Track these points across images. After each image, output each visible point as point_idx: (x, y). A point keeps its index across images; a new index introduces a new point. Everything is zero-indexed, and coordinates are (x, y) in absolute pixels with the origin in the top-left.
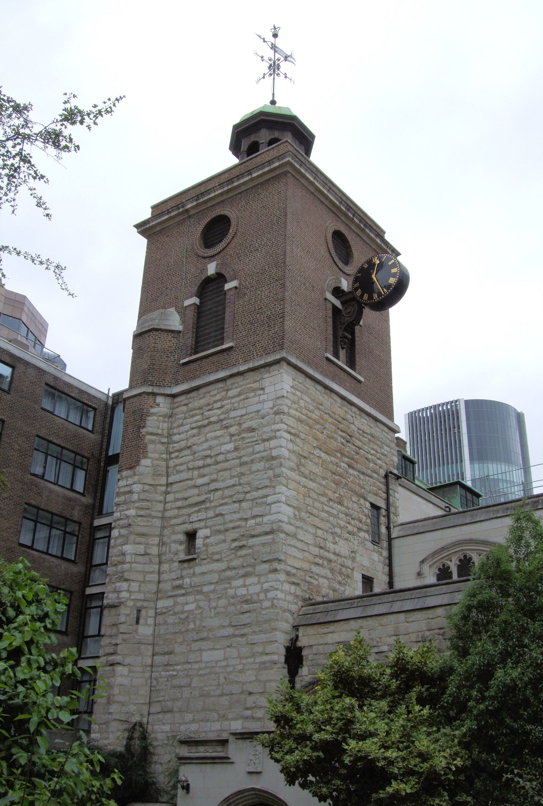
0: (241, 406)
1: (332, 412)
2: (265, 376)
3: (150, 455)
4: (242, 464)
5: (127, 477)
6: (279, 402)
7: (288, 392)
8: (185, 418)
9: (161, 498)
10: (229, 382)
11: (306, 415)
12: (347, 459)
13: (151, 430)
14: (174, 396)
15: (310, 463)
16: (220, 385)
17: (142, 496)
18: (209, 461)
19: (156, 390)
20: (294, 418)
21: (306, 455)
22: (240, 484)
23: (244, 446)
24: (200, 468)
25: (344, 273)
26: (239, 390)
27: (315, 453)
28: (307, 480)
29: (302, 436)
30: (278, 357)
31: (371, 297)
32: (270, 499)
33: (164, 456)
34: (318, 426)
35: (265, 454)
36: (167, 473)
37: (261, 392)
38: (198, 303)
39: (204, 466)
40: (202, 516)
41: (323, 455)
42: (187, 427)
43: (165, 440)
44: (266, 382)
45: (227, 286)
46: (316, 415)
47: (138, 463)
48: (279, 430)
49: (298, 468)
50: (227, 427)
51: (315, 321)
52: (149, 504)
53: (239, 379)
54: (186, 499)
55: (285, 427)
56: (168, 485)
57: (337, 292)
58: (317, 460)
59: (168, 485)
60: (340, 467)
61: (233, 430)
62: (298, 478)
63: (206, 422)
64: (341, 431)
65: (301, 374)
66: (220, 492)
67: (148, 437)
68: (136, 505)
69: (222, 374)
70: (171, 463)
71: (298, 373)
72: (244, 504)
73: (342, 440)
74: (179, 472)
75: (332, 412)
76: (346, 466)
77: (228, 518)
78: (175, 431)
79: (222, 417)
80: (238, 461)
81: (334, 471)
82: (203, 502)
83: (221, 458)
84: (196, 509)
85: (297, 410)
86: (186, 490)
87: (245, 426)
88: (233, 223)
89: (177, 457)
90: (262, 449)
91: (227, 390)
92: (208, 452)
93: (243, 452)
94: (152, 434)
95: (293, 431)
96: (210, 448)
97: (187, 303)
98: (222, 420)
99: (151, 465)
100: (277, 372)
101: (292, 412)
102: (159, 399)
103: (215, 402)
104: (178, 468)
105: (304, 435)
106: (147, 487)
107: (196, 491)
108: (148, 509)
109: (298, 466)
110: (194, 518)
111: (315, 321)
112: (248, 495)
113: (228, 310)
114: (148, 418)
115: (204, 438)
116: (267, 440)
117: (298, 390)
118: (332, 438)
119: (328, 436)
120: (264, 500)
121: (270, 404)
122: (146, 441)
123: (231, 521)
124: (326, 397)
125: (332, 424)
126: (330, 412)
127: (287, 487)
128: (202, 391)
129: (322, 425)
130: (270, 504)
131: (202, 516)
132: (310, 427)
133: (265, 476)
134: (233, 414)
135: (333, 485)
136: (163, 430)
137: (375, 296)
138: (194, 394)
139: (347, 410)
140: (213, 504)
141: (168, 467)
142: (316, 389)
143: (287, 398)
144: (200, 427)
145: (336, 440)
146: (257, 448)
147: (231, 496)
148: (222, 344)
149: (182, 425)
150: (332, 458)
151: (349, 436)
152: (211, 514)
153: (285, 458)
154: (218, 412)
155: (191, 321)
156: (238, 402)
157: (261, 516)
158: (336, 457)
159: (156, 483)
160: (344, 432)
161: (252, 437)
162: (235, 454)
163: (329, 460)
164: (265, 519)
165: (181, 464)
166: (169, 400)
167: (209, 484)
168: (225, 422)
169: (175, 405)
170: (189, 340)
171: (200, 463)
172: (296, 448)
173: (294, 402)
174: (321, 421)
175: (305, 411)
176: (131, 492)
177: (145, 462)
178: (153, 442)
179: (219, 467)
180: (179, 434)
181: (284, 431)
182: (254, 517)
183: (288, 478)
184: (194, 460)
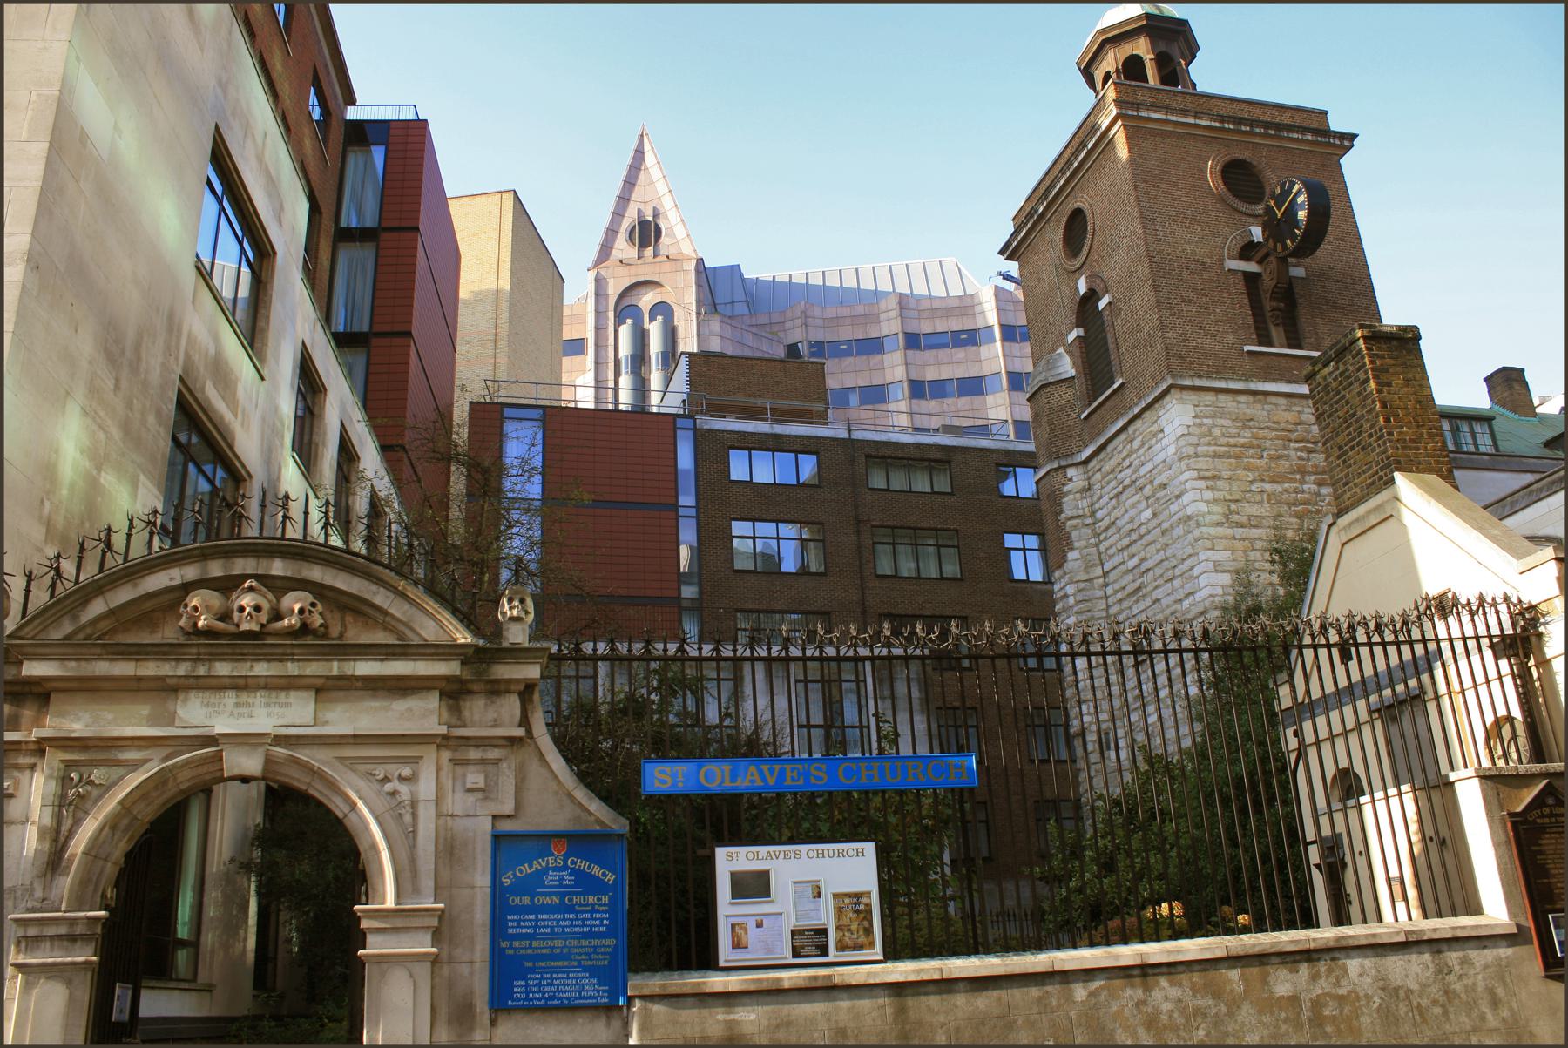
0: (1148, 458)
1: (1274, 422)
2: (1161, 414)
3: (1076, 545)
4: (1164, 533)
5: (1060, 579)
6: (1182, 442)
7: (1189, 426)
8: (1102, 488)
9: (1101, 593)
10: (1131, 429)
11: (1228, 445)
12: (1313, 478)
13: (1069, 514)
14: (1086, 462)
15: (1247, 505)
16: (1123, 436)
17: (1079, 597)
18: (1134, 536)
19: (1063, 463)
20: (1207, 456)
21: (1238, 497)
22: (1167, 559)
23: (1161, 508)
24: (1128, 546)
25: (1256, 216)
26: (1141, 438)
27: (1253, 489)
28: (1247, 529)
29: (1226, 474)
30: (1164, 386)
31: (1285, 247)
32: (1196, 572)
33: (1093, 541)
34: (1252, 451)
35: (1181, 514)
36: (1101, 560)
37: (1161, 435)
38: (1082, 334)
39: (1131, 544)
40: (1141, 606)
41: (1268, 487)
42: (1106, 499)
43: (1088, 521)
44: (1163, 422)
45: (1102, 304)
46: (1244, 437)
47: (1064, 559)
48: (1187, 481)
49: (1228, 519)
50: (1141, 489)
51: (1218, 310)
52: (1089, 604)
53: (1138, 423)
54: (1124, 588)
55: (1195, 474)
56: (1105, 575)
57: (1247, 250)
58: (1259, 498)
59: (1105, 575)
60: (1303, 492)
61: (1147, 491)
62: (1229, 532)
63: (1121, 487)
64: (1297, 441)
65: (1206, 393)
66: (1151, 572)
67: (1069, 523)
68: (1076, 609)
69: (1120, 424)
70: (1102, 548)
71: (1202, 394)
72: (1177, 583)
73: (1299, 453)
74: (1111, 557)
75: (1274, 422)
76: (1315, 487)
77: (1164, 602)
78: (1097, 506)
79: (1133, 478)
80: (1158, 530)
81: (1292, 501)
82: (1139, 588)
83: (1143, 530)
84: (1135, 598)
85: (1209, 444)
86: (1121, 577)
87: (1156, 483)
88: (1089, 217)
89: (1106, 539)
90: (1177, 509)
91: (1131, 441)
92: (1130, 526)
93: (1161, 518)
94: (1072, 518)
95: (1208, 474)
96: (1132, 520)
97: (1071, 337)
98: (1134, 482)
99: (1079, 557)
100: (1170, 405)
101: (1201, 449)
102: (1071, 472)
103: (1124, 459)
104: (1111, 552)
105: (1229, 473)
106: (1082, 585)
107: (1130, 577)
108: (1089, 611)
109: (1226, 516)
110: (1135, 611)
111: (1218, 310)
112: (1176, 570)
113: (1109, 336)
114: (1064, 500)
115: (1123, 510)
116: (1178, 497)
117: (1207, 417)
118: (1280, 457)
119: (1271, 458)
120: (1191, 573)
121: (1172, 449)
122: (1068, 529)
123: (1168, 606)
124: (1259, 406)
125: (1278, 438)
126: (1269, 424)
127: (1213, 549)
128: (1110, 447)
129: (1259, 447)
130: (1197, 577)
131: (1141, 606)
132: (1236, 458)
133: (1186, 543)
134: (1144, 470)
135: (1294, 520)
136: (1083, 509)
137: (1289, 242)
138: (1102, 455)
139: (1300, 409)
140: (1148, 589)
141: (1100, 554)
142: (1239, 402)
143: (1189, 434)
144: (1117, 496)
145: (1288, 457)
146: (1174, 508)
147: (1162, 575)
148: (1114, 383)
149: (1101, 497)
150: (1286, 485)
151: (1313, 443)
152: (1148, 602)
153: (1203, 515)
154: (1128, 471)
155: (1080, 360)
156: (1144, 455)
157: (1193, 593)
158: (1292, 480)
159: (1092, 576)
160: (1301, 441)
161: (1166, 495)
162: (1155, 522)
163: (1280, 489)
164: (1197, 595)
165: (1111, 547)
166: (1081, 469)
167: (1139, 565)
168: (1138, 483)
169: (1090, 473)
170: (1081, 387)
171: (1126, 541)
172: (1219, 495)
173: (1203, 436)
174: (1255, 442)
175: (1224, 440)
176: (1066, 596)
177: (1071, 555)
178: (1075, 527)
179: (1144, 542)
180: (1101, 509)
181: (1195, 479)
182: (1187, 596)
183: (1212, 539)
184: (1120, 539)
